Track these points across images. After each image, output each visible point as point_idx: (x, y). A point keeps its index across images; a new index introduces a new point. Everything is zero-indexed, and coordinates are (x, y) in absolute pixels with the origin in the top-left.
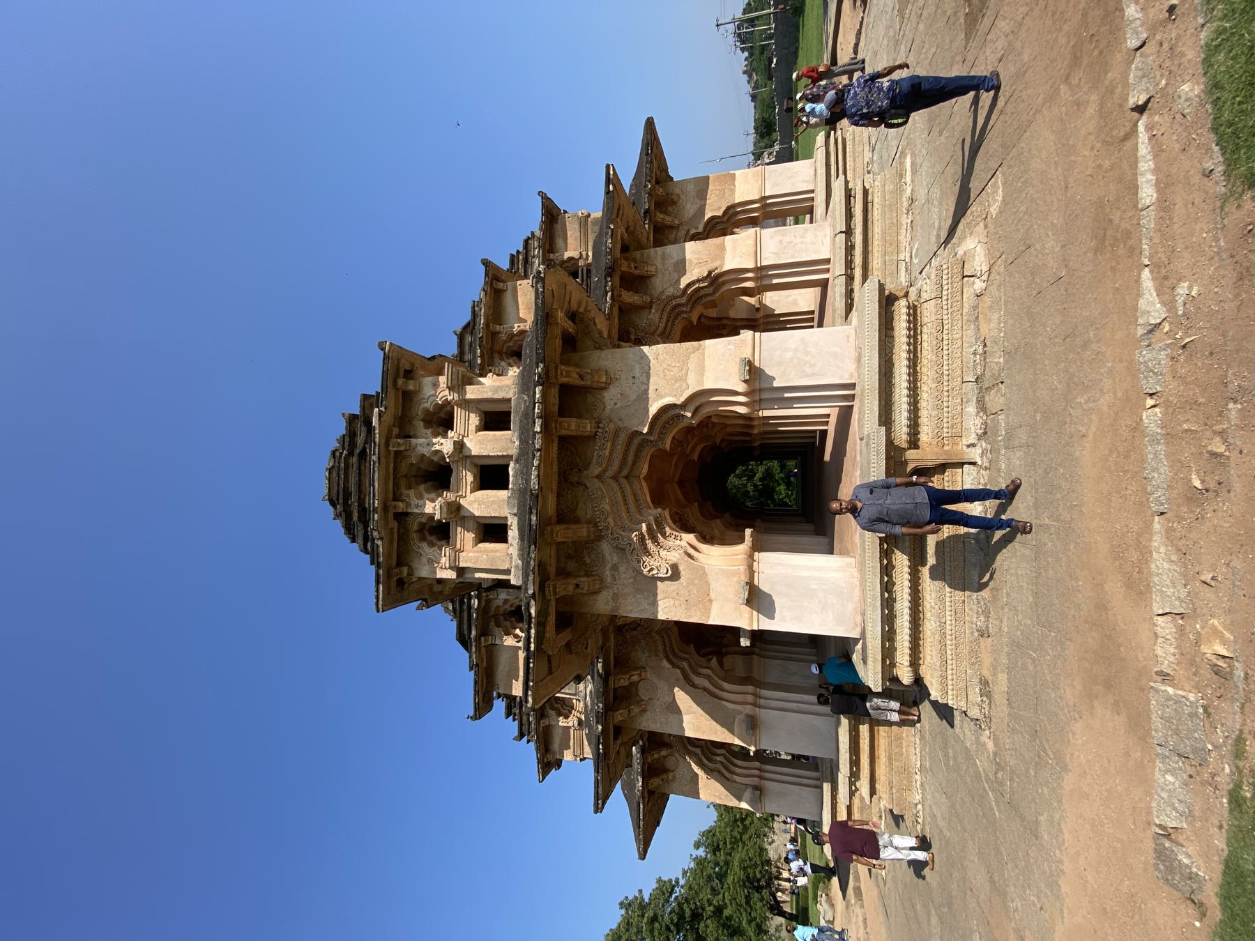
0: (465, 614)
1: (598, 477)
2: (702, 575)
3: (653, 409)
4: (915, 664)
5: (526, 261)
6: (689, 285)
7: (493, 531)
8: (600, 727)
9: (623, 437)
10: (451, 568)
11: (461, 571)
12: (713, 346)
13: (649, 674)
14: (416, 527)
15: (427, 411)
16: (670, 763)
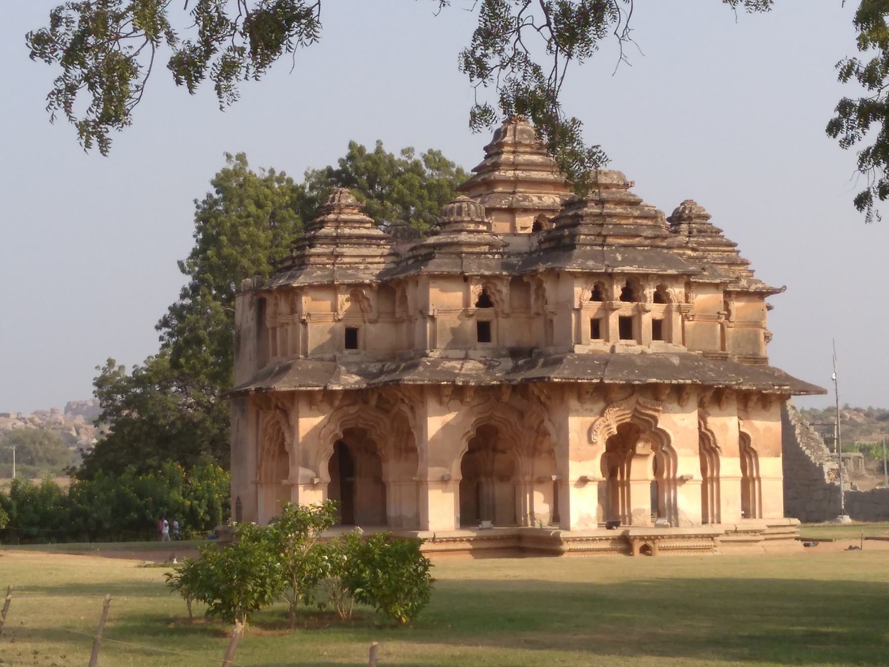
0: (477, 250)
1: (637, 402)
2: (593, 457)
3: (668, 431)
4: (570, 551)
5: (732, 264)
6: (712, 433)
7: (597, 329)
8: (461, 384)
9: (656, 414)
10: (581, 305)
11: (578, 311)
12: (696, 462)
13: (465, 409)
14: (602, 280)
15: (665, 288)
16: (325, 407)
